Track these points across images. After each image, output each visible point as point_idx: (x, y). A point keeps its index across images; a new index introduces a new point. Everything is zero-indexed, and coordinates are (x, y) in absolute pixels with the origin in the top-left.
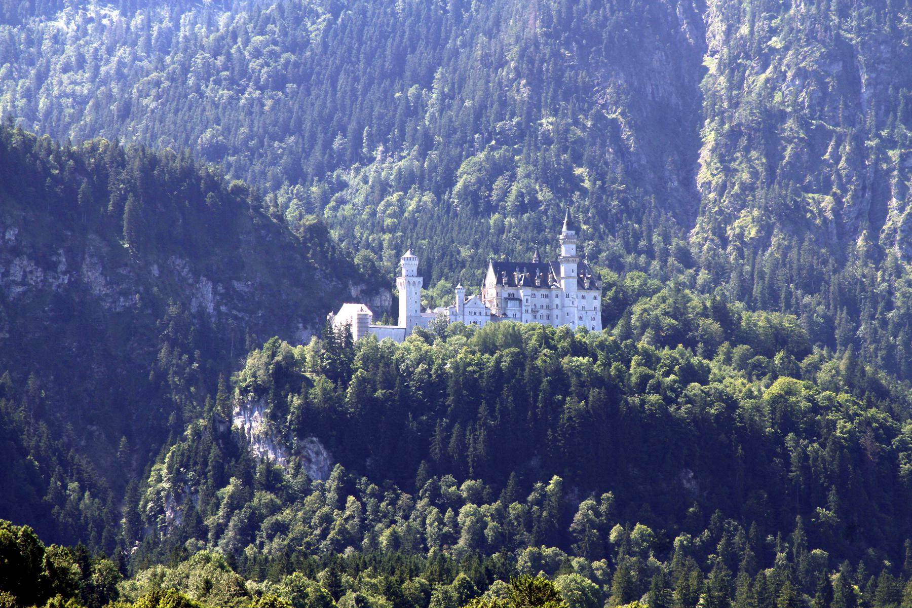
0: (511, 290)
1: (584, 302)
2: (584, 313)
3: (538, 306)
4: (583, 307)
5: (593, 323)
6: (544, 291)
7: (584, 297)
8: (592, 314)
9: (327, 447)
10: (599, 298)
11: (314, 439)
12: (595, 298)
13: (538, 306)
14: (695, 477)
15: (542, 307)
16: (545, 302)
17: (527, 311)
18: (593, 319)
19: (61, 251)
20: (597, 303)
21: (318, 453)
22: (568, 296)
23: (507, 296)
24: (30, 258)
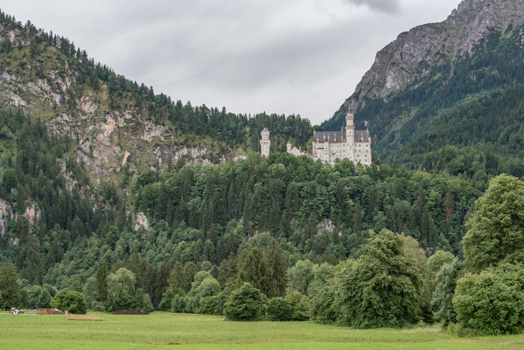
0: (321, 144)
1: (360, 148)
2: (360, 153)
4: (360, 151)
5: (366, 158)
6: (338, 144)
7: (360, 146)
8: (364, 154)
9: (147, 218)
10: (369, 146)
11: (142, 213)
12: (367, 146)
14: (332, 224)
16: (339, 149)
17: (326, 154)
18: (366, 156)
19: (223, 156)
20: (369, 148)
21: (143, 220)
24: (209, 159)
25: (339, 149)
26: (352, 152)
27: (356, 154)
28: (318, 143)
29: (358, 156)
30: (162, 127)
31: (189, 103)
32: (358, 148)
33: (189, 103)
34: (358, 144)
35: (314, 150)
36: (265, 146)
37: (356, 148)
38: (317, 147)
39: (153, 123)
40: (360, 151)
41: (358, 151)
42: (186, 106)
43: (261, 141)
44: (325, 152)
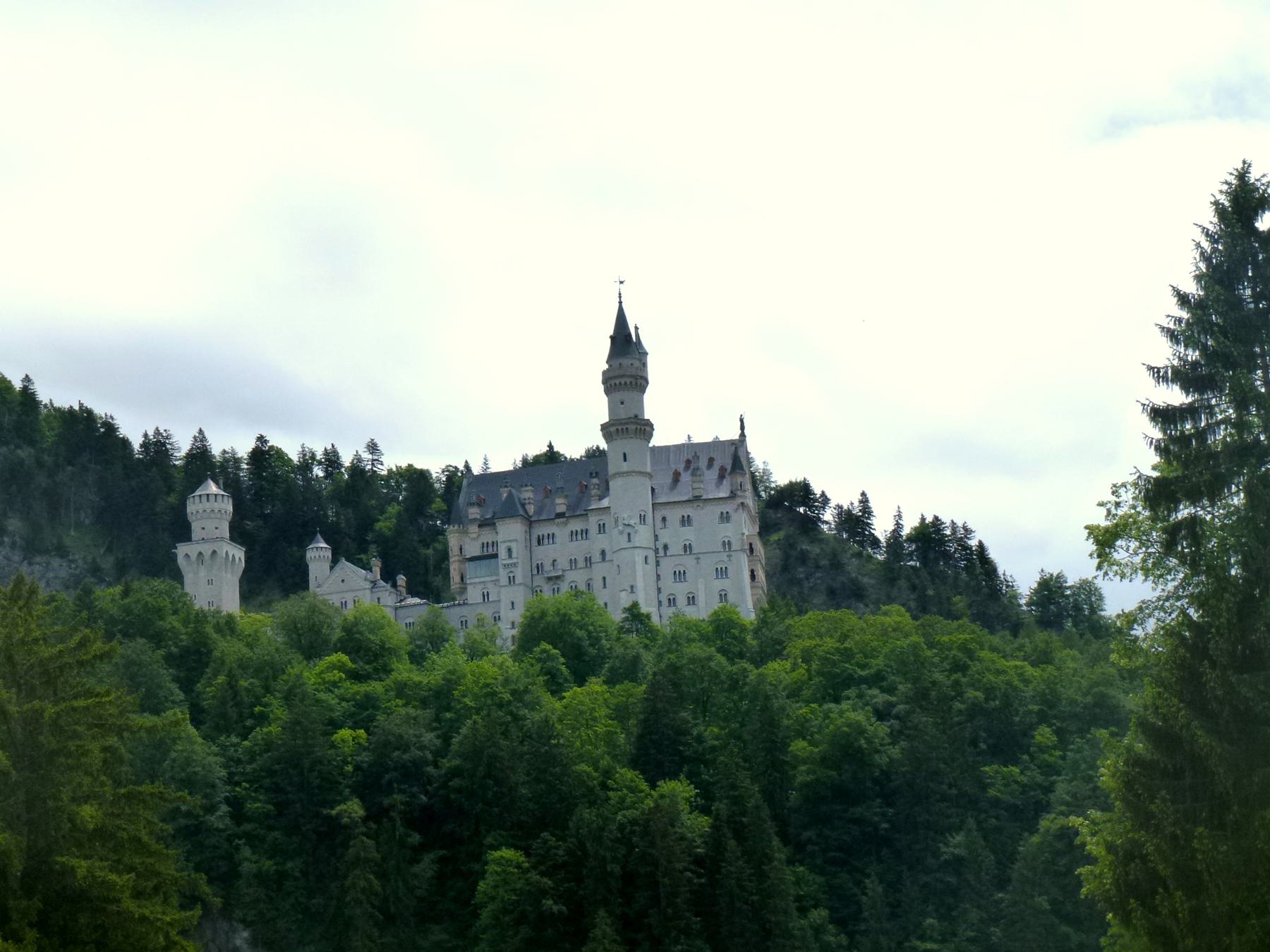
0: (487, 536)
1: (688, 534)
2: (689, 561)
3: (563, 563)
4: (687, 548)
6: (576, 525)
7: (686, 521)
8: (709, 564)
12: (725, 518)
13: (563, 563)
15: (573, 563)
16: (578, 549)
17: (511, 580)
18: (722, 573)
22: (616, 521)
23: (477, 553)
25: (578, 549)
26: (639, 557)
27: (668, 566)
28: (474, 529)
29: (680, 576)
30: (56, 562)
31: (201, 437)
32: (675, 536)
33: (201, 437)
34: (674, 515)
35: (454, 569)
36: (203, 573)
37: (665, 537)
38: (473, 549)
39: (13, 546)
40: (687, 548)
41: (676, 548)
42: (191, 456)
43: (182, 550)
44: (503, 575)
